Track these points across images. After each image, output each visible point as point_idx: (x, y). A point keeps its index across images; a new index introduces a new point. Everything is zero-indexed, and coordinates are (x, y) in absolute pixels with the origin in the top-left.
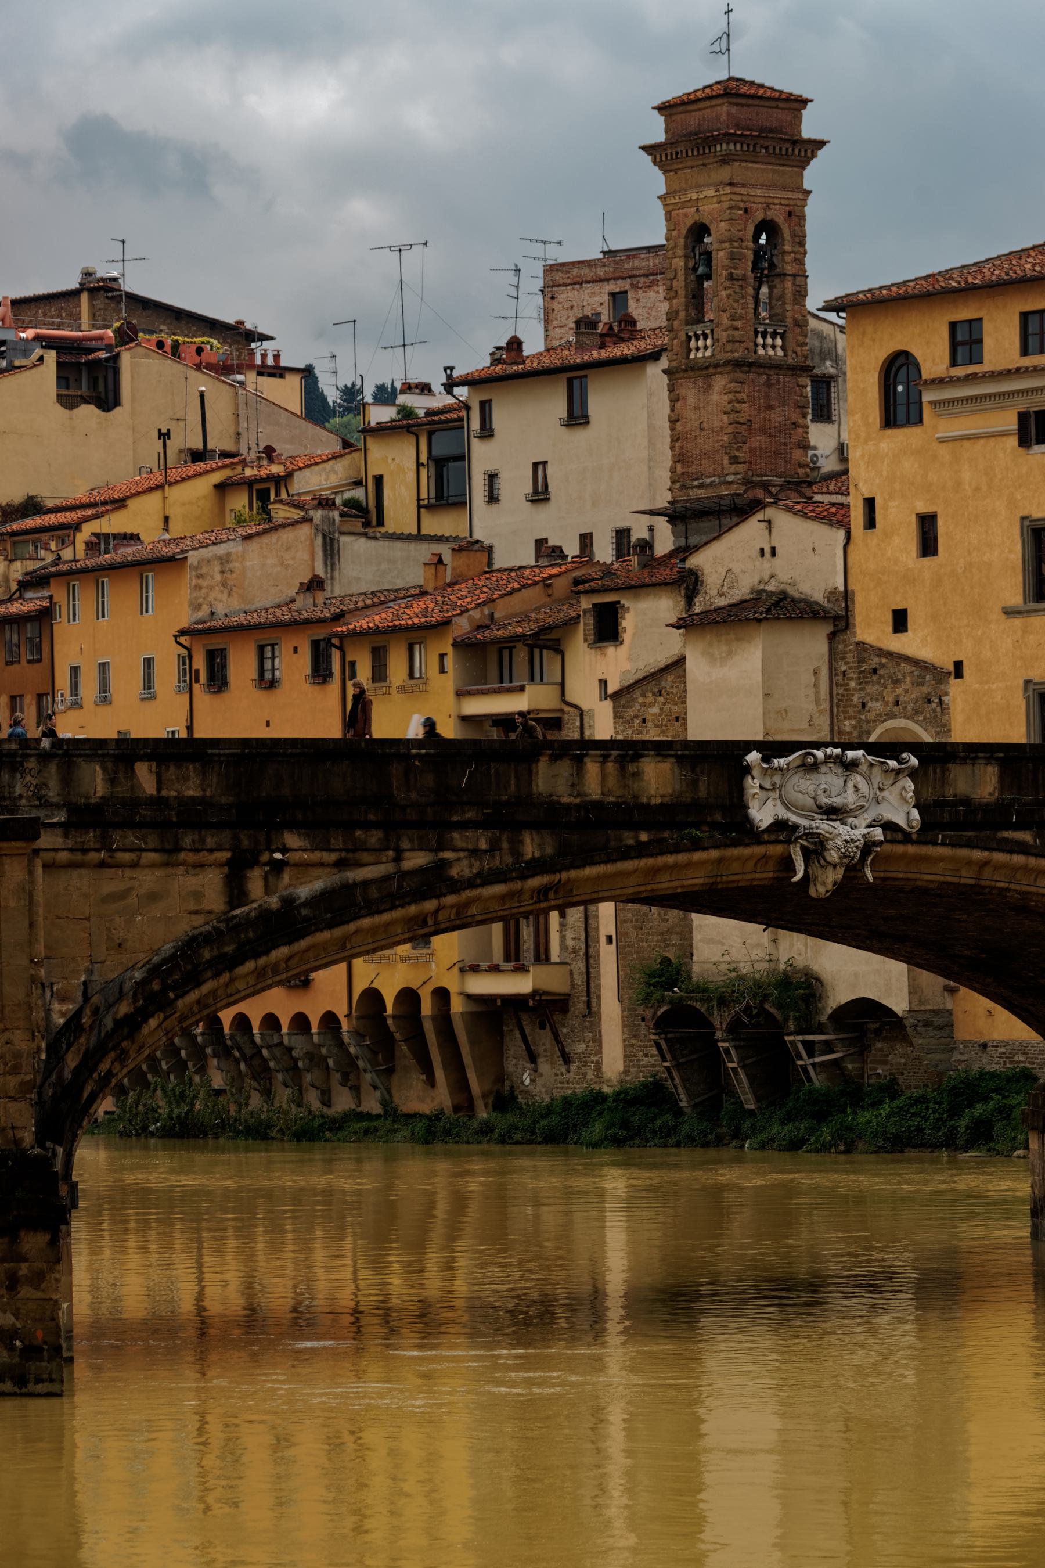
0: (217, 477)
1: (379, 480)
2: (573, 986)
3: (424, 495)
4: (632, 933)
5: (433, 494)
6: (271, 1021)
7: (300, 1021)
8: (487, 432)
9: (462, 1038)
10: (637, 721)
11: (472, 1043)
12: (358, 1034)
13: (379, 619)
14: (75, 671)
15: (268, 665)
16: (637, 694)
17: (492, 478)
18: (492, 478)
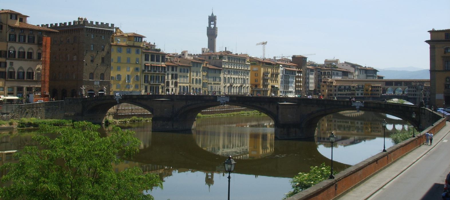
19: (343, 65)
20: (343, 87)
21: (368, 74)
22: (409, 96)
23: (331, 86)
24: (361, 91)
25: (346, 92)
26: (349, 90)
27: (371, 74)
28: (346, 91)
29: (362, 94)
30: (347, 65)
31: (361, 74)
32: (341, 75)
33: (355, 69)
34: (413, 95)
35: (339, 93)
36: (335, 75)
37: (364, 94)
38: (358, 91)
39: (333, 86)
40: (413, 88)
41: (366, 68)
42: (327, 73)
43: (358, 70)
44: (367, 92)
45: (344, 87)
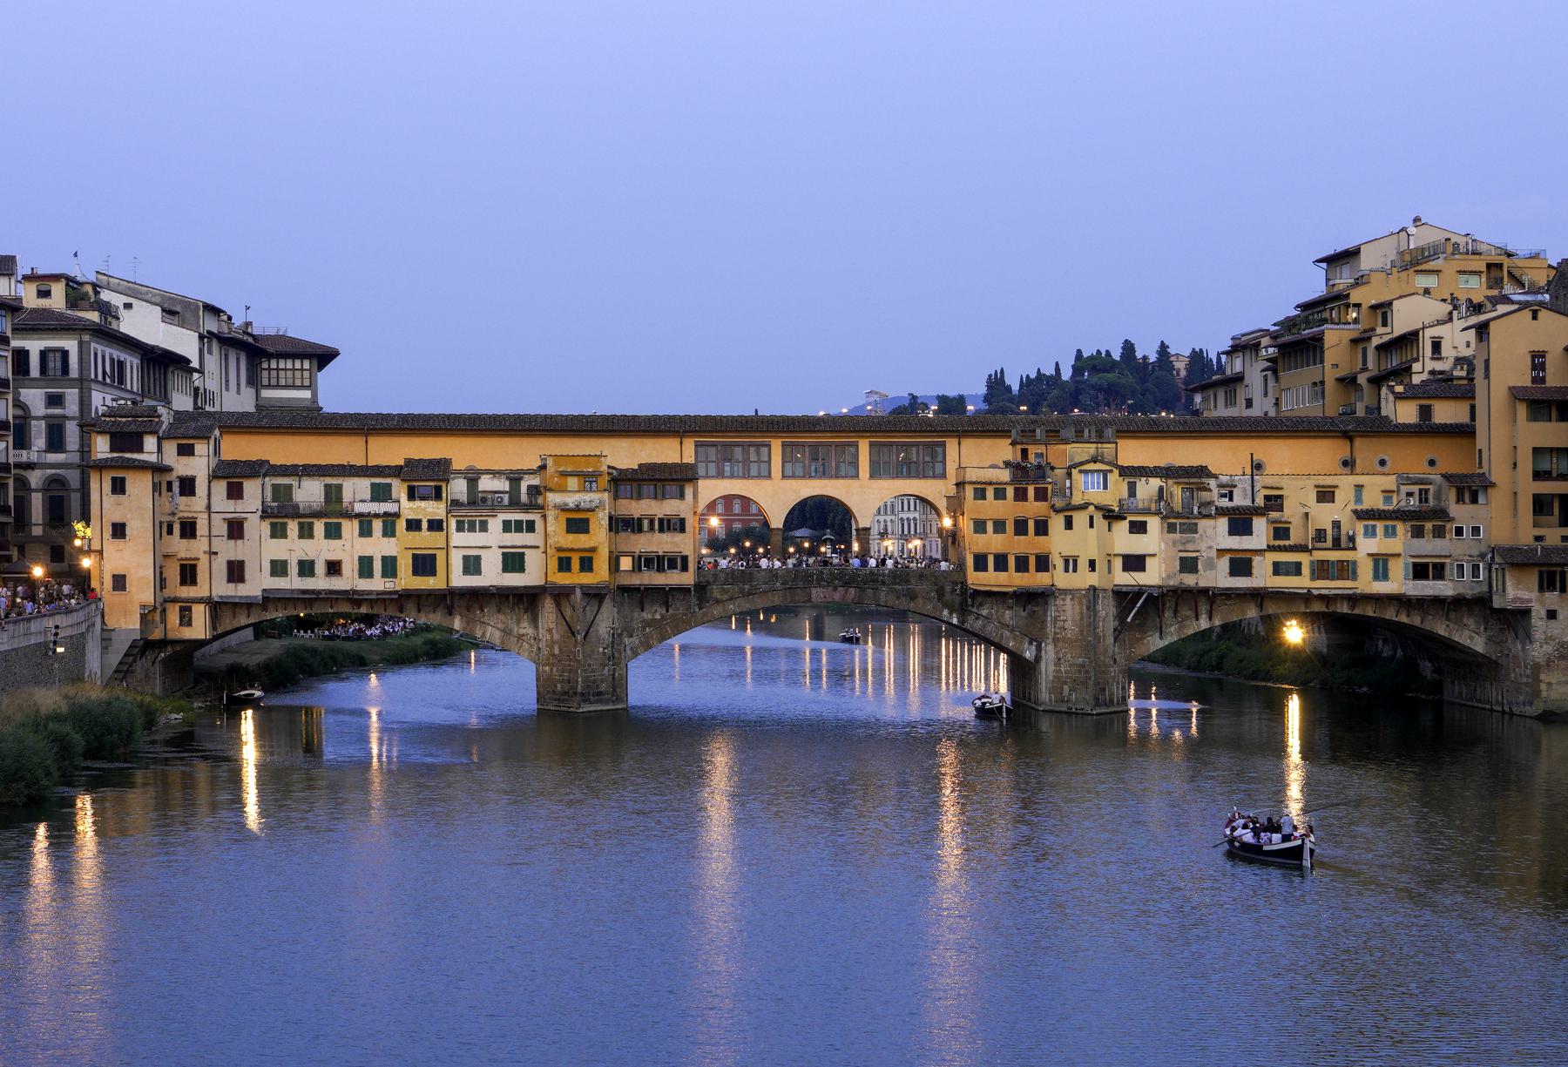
20: (309, 492)
21: (267, 394)
22: (975, 579)
23: (188, 486)
24: (507, 526)
25: (350, 546)
26: (377, 525)
27: (294, 387)
28: (350, 528)
29: (513, 562)
30: (128, 306)
31: (227, 381)
32: (135, 390)
33: (201, 337)
34: (1022, 564)
36: (108, 380)
37: (564, 565)
38: (472, 529)
39: (214, 476)
40: (1021, 495)
42: (34, 360)
43: (215, 344)
44: (581, 541)
45: (326, 486)
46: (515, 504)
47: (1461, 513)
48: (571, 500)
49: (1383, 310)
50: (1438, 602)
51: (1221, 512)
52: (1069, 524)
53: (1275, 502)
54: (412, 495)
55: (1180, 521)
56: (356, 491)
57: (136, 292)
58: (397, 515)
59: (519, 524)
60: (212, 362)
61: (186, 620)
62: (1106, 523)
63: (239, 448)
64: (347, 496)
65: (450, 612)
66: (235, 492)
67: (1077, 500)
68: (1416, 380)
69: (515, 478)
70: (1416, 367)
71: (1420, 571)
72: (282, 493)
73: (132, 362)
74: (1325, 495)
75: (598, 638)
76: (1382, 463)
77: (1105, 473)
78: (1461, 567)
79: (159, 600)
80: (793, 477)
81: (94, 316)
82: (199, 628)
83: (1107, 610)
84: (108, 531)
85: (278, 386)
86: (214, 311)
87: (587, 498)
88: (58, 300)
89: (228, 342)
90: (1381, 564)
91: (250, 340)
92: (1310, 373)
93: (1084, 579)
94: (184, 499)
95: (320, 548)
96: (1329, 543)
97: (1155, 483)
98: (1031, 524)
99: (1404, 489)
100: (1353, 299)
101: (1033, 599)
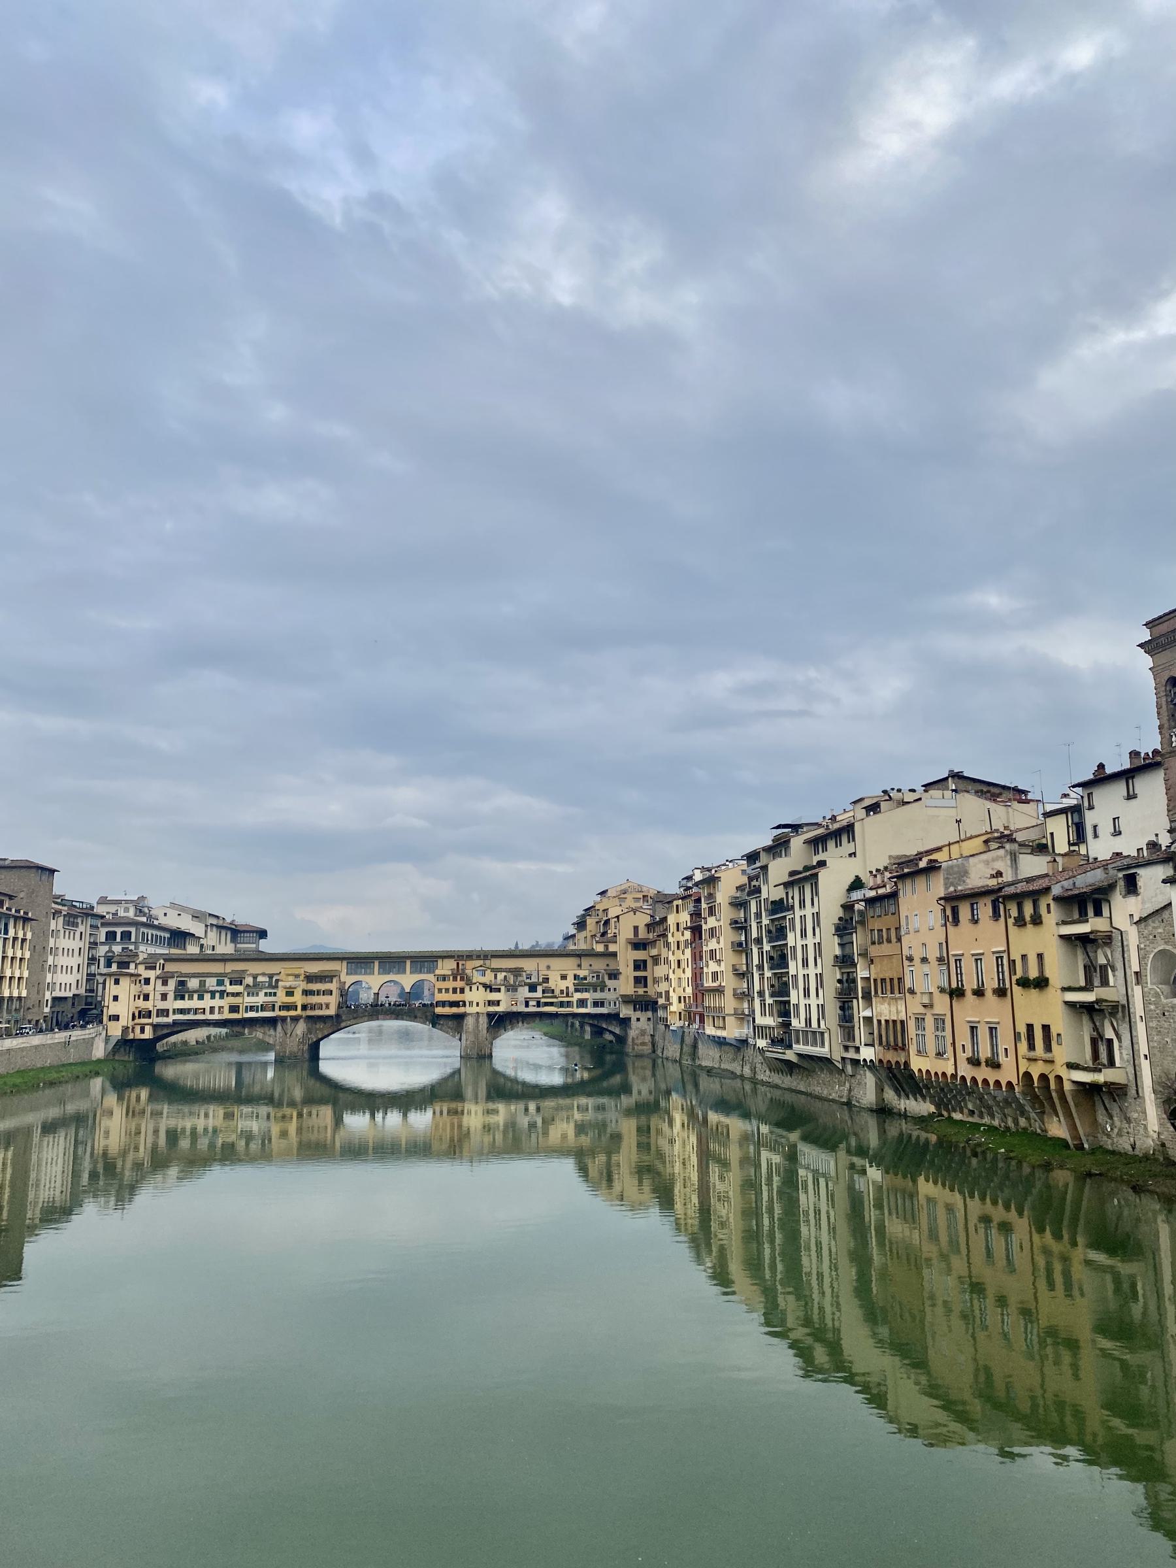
0: (984, 838)
1: (1052, 834)
2: (1128, 1079)
3: (1071, 839)
4: (1158, 1054)
5: (1075, 838)
6: (985, 1081)
7: (997, 1083)
8: (1091, 808)
9: (1072, 1104)
10: (1151, 937)
11: (1076, 1105)
12: (1024, 1093)
13: (1021, 888)
14: (907, 917)
15: (975, 913)
16: (1150, 921)
17: (1095, 827)
18: (1095, 827)
19: (165, 914)
23: (147, 981)
24: (266, 994)
25: (207, 1002)
26: (217, 995)
27: (249, 943)
28: (207, 996)
30: (179, 915)
33: (206, 926)
35: (180, 1004)
38: (253, 995)
39: (158, 977)
40: (455, 979)
41: (236, 926)
43: (214, 929)
45: (200, 981)
46: (270, 986)
47: (610, 983)
48: (288, 984)
49: (606, 911)
50: (601, 1016)
51: (526, 984)
52: (471, 990)
53: (546, 980)
54: (231, 984)
55: (512, 988)
56: (211, 983)
57: (181, 909)
58: (225, 991)
59: (270, 993)
60: (213, 935)
61: (142, 1031)
62: (484, 989)
63: (170, 967)
64: (207, 985)
65: (244, 1027)
66: (165, 983)
67: (474, 981)
68: (609, 935)
69: (271, 976)
70: (609, 931)
71: (596, 1004)
72: (182, 983)
73: (167, 935)
74: (564, 977)
75: (297, 1035)
76: (591, 965)
77: (485, 971)
78: (610, 1003)
79: (130, 1024)
80: (382, 974)
81: (144, 919)
82: (148, 1034)
83: (483, 1021)
84: (112, 998)
85: (244, 943)
86: (218, 917)
87: (293, 984)
88: (131, 914)
89: (218, 927)
90: (582, 1003)
91: (234, 927)
92: (583, 934)
93: (473, 1010)
94: (146, 986)
95: (195, 1003)
96: (565, 995)
97: (504, 974)
98: (458, 990)
99: (591, 975)
100: (596, 908)
101: (460, 1017)
